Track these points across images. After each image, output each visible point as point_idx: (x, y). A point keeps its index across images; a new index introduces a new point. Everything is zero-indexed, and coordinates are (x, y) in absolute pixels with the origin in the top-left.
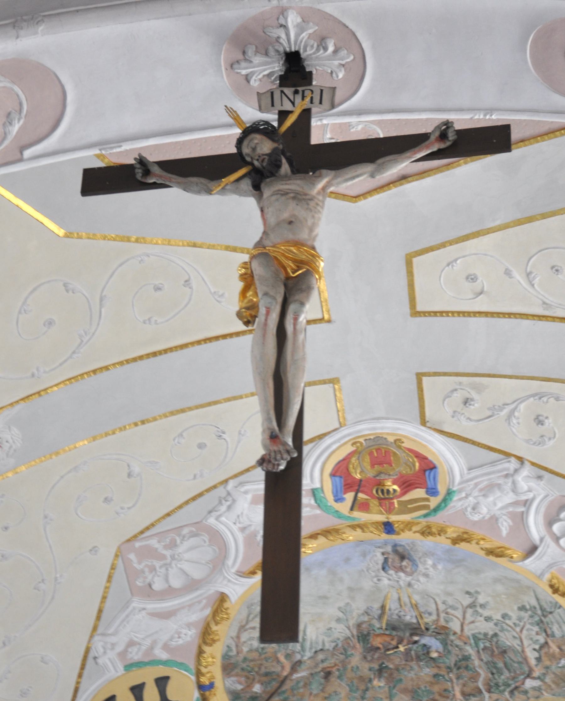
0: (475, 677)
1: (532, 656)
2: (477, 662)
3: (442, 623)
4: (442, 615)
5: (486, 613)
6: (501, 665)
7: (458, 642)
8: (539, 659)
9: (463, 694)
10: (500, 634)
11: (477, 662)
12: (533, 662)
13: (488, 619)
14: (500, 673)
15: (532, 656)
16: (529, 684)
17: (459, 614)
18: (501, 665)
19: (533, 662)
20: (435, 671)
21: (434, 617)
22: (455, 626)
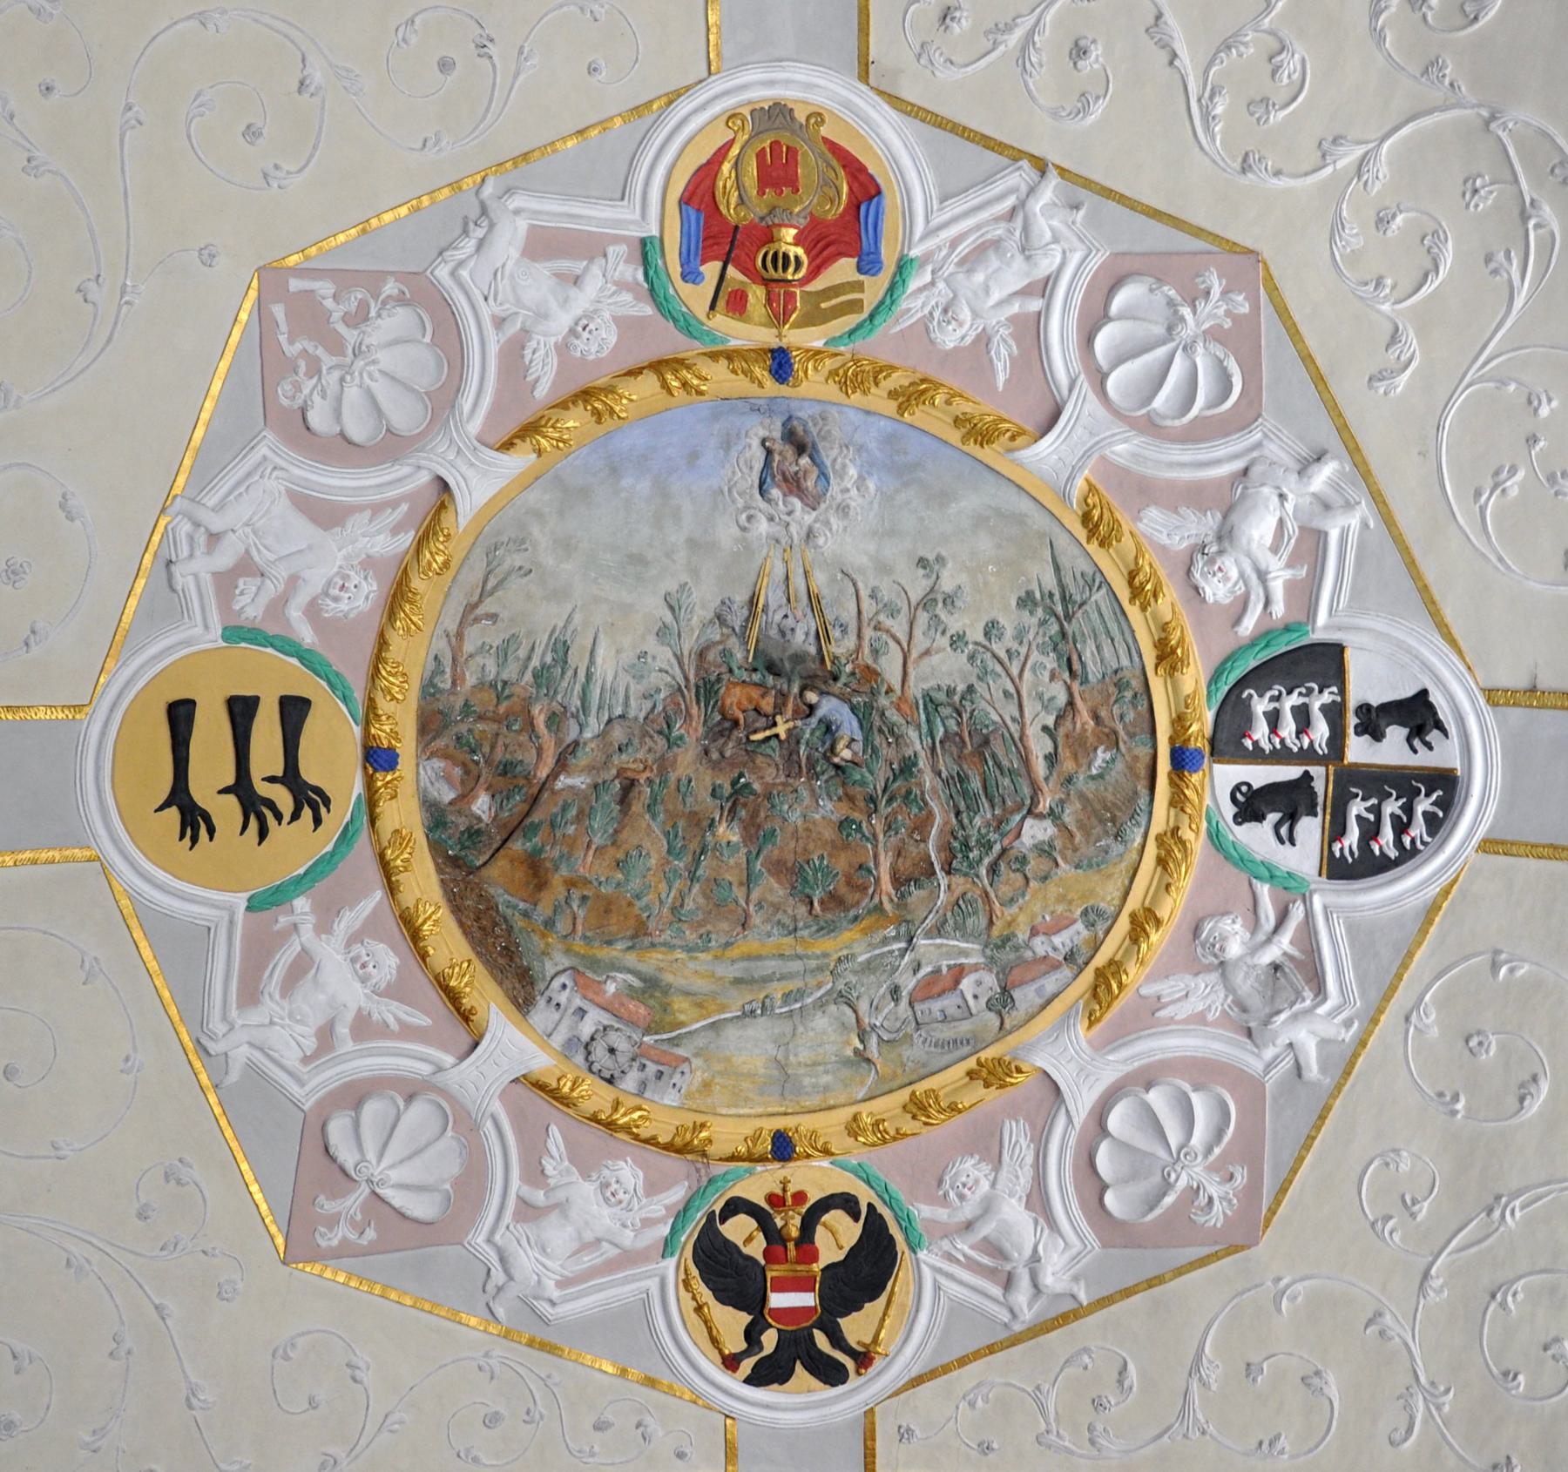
0: (921, 827)
1: (1039, 746)
2: (928, 780)
3: (866, 657)
4: (868, 633)
5: (955, 623)
6: (976, 784)
7: (893, 716)
8: (1052, 759)
9: (897, 881)
10: (980, 688)
11: (928, 780)
12: (1040, 768)
13: (957, 641)
14: (974, 809)
15: (1039, 746)
16: (1035, 832)
17: (899, 627)
18: (976, 784)
19: (1040, 768)
20: (843, 810)
21: (850, 642)
22: (891, 668)
